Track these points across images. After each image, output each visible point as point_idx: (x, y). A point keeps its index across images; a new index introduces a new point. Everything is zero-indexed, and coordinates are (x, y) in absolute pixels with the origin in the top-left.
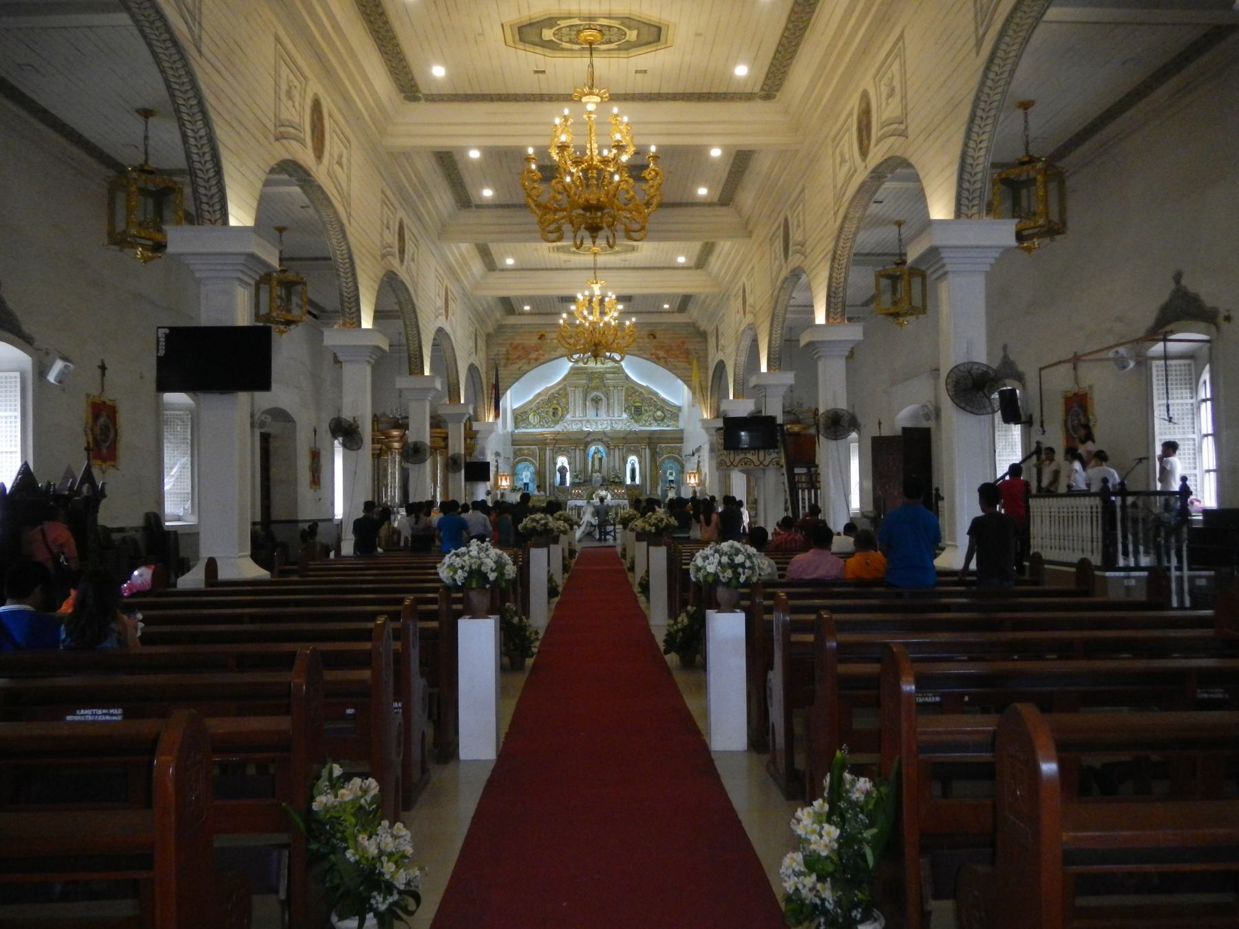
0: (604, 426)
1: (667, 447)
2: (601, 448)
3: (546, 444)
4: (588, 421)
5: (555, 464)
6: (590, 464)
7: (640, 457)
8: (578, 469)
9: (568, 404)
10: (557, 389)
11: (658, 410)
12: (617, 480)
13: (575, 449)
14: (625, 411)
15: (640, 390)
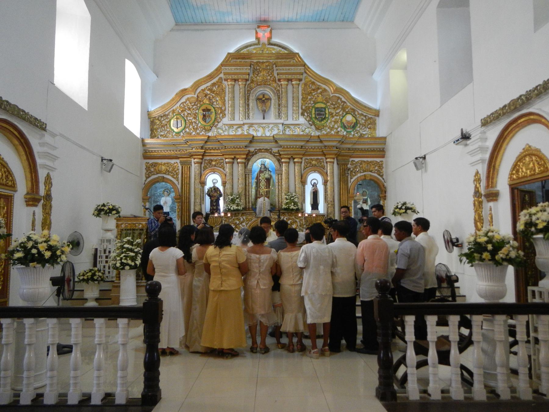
0: (275, 132)
1: (362, 161)
2: (269, 162)
3: (191, 156)
4: (251, 125)
5: (203, 184)
6: (254, 186)
7: (324, 174)
8: (235, 191)
9: (224, 104)
10: (209, 84)
11: (347, 113)
12: (292, 207)
13: (233, 163)
14: (303, 114)
15: (324, 86)
